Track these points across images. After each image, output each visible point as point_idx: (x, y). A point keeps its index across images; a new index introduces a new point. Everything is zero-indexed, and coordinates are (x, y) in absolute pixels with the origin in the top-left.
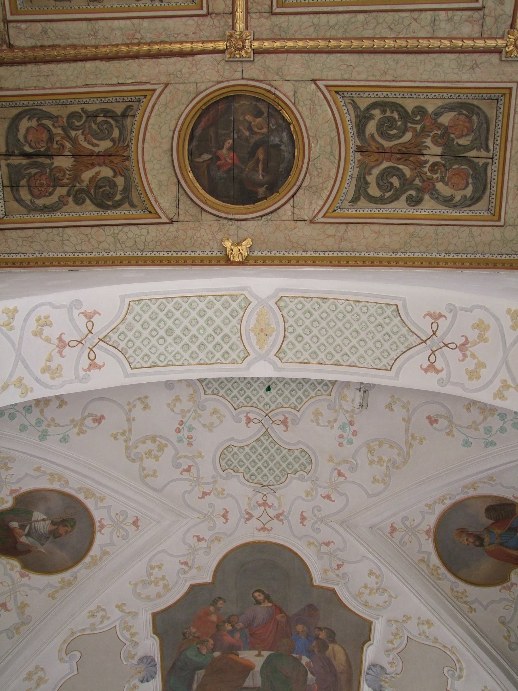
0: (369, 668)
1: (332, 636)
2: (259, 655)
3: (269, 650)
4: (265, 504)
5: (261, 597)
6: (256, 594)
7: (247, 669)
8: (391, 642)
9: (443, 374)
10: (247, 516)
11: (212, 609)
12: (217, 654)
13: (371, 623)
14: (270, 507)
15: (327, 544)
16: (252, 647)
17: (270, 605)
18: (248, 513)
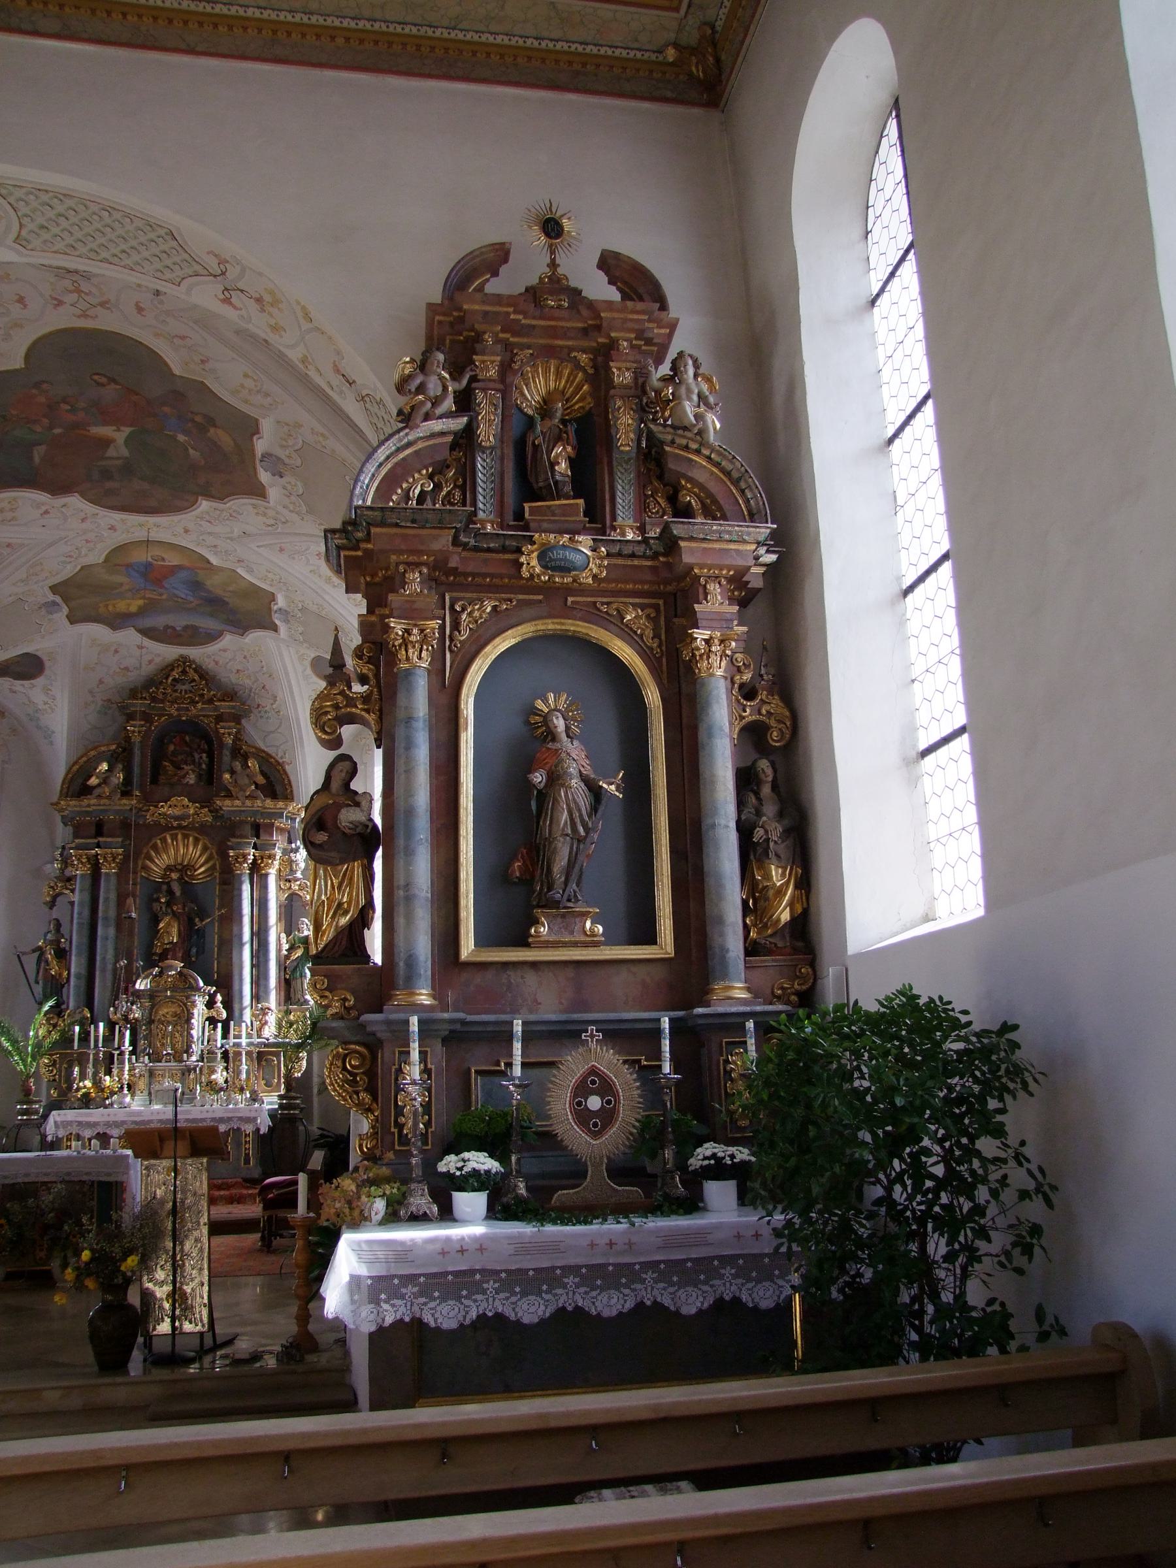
0: (263, 456)
1: (211, 422)
2: (118, 430)
3: (131, 426)
4: (78, 291)
5: (104, 380)
6: (96, 377)
7: (107, 442)
8: (285, 440)
9: (243, 312)
10: (56, 302)
11: (34, 391)
12: (57, 431)
13: (257, 421)
14: (86, 294)
15: (183, 338)
16: (105, 423)
17: (118, 387)
18: (56, 299)
